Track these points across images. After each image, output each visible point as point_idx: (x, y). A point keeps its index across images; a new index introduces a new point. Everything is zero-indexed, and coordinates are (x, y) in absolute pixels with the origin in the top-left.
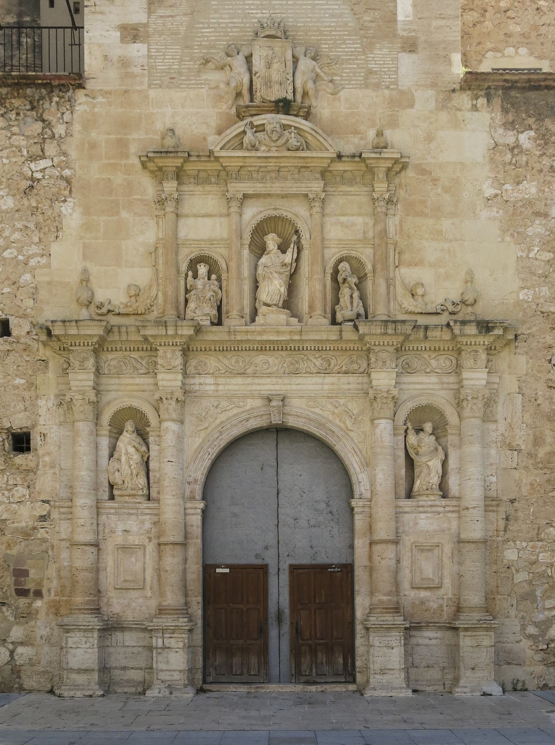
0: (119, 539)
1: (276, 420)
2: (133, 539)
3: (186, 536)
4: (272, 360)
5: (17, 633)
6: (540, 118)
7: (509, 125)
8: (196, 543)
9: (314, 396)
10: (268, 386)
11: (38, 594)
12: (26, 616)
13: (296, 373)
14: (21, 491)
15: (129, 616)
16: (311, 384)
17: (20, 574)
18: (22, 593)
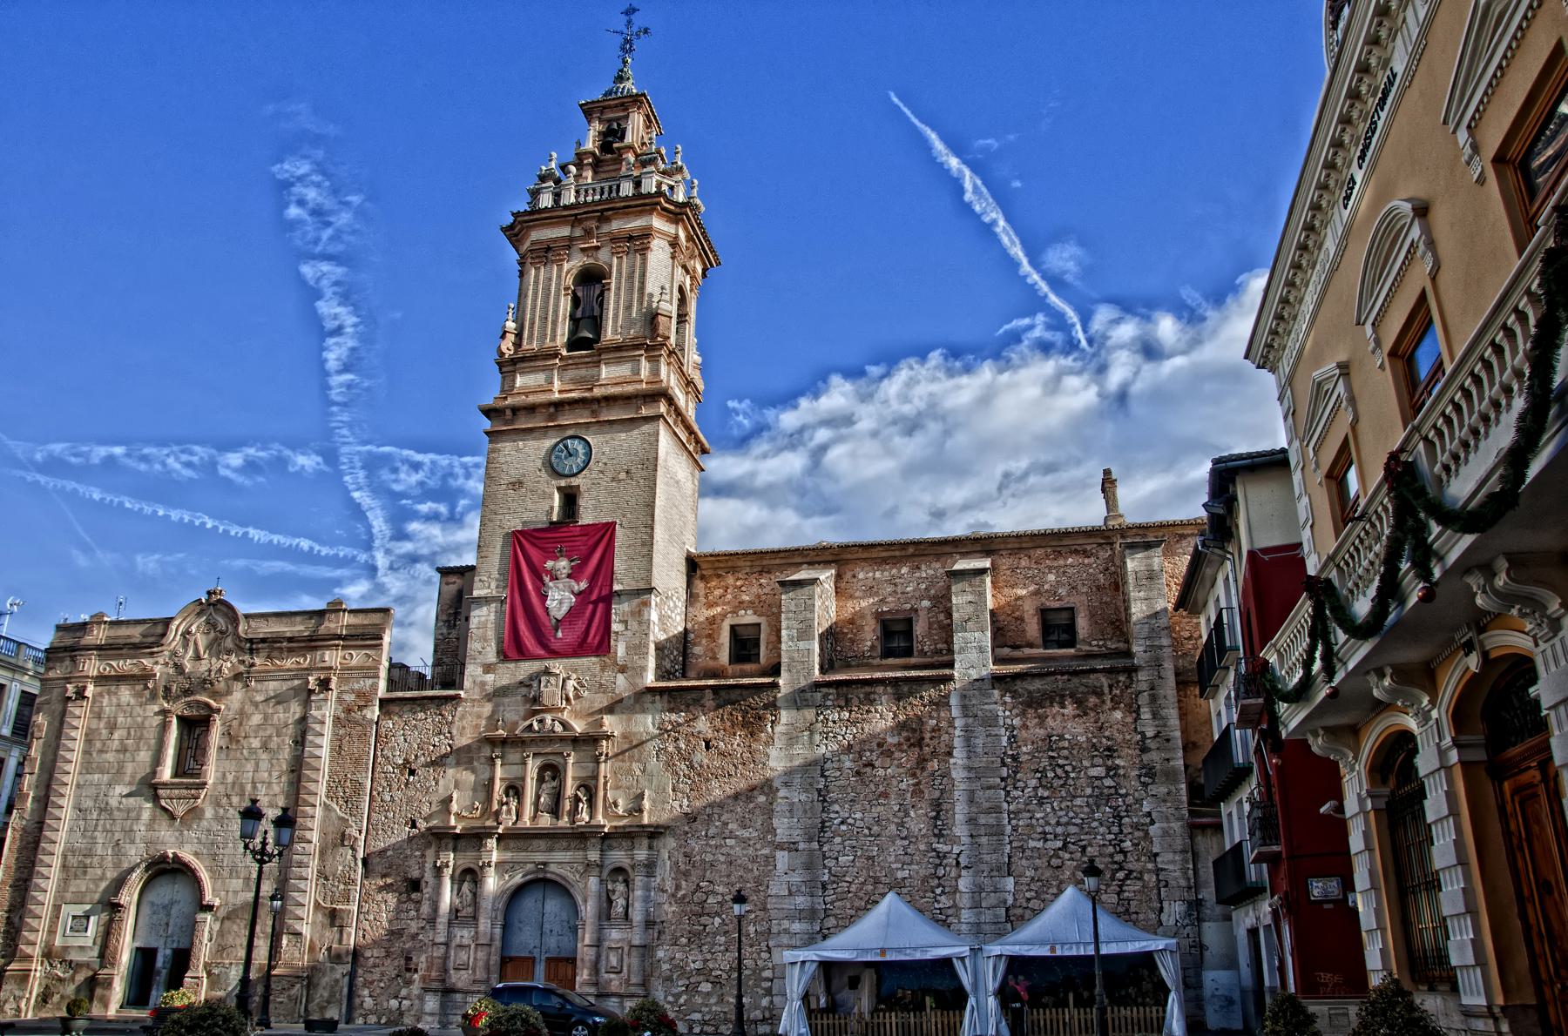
0: (457, 940)
1: (541, 876)
2: (465, 942)
3: (492, 939)
4: (542, 843)
5: (404, 992)
6: (688, 706)
7: (671, 710)
8: (498, 943)
9: (561, 862)
10: (540, 857)
11: (416, 971)
12: (409, 983)
13: (551, 850)
14: (413, 913)
15: (460, 985)
16: (559, 856)
17: (408, 959)
18: (408, 970)
